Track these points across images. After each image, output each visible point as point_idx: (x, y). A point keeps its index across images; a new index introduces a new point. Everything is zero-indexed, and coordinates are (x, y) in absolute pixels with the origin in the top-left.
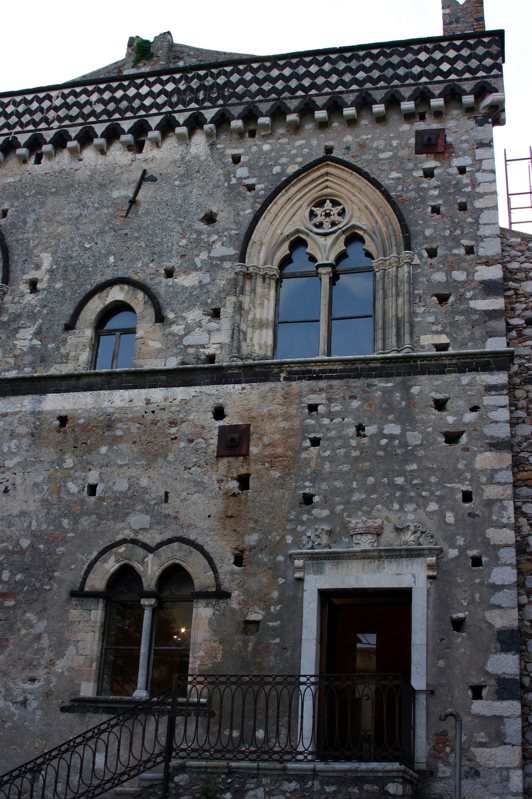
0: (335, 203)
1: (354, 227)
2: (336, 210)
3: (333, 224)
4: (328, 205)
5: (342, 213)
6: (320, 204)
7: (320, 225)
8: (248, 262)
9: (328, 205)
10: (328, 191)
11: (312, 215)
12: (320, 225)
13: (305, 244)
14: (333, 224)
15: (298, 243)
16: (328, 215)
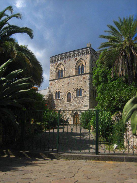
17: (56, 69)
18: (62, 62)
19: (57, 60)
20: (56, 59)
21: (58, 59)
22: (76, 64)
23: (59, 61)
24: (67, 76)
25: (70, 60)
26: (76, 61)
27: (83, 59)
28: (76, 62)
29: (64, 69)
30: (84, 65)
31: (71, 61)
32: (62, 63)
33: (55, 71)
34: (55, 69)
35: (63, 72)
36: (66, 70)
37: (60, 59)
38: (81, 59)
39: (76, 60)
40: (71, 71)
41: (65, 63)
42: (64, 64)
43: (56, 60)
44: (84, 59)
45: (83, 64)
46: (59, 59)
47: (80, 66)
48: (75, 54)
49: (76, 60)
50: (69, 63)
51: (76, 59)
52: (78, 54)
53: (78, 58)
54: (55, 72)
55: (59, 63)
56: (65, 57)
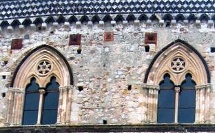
0: (181, 60)
1: (189, 71)
2: (181, 63)
3: (181, 69)
4: (178, 61)
5: (184, 64)
6: (175, 60)
7: (175, 69)
8: (148, 83)
9: (178, 61)
10: (178, 55)
11: (172, 64)
12: (175, 69)
13: (169, 76)
14: (181, 69)
15: (167, 75)
16: (178, 64)
17: (15, 74)
18: (59, 36)
19: (27, 23)
20: (21, 20)
21: (33, 20)
22: (146, 67)
23: (40, 29)
24: (85, 122)
25: (109, 37)
26: (147, 49)
27: (191, 49)
28: (150, 57)
29: (72, 82)
30: (200, 80)
31: (116, 48)
32: (59, 49)
33: (6, 81)
34: (8, 74)
35: (63, 97)
36: (81, 89)
37: (50, 21)
38: (179, 41)
39: (152, 46)
40: (114, 99)
41: (79, 52)
42: (69, 51)
43: (16, 24)
44: (199, 47)
45: (189, 75)
46: (39, 21)
47: (177, 79)
48: (149, 15)
49: (152, 46)
50: (106, 54)
51: (151, 38)
52: (168, 18)
53: (166, 36)
54: (5, 90)
55: (35, 40)
56: (79, 17)
